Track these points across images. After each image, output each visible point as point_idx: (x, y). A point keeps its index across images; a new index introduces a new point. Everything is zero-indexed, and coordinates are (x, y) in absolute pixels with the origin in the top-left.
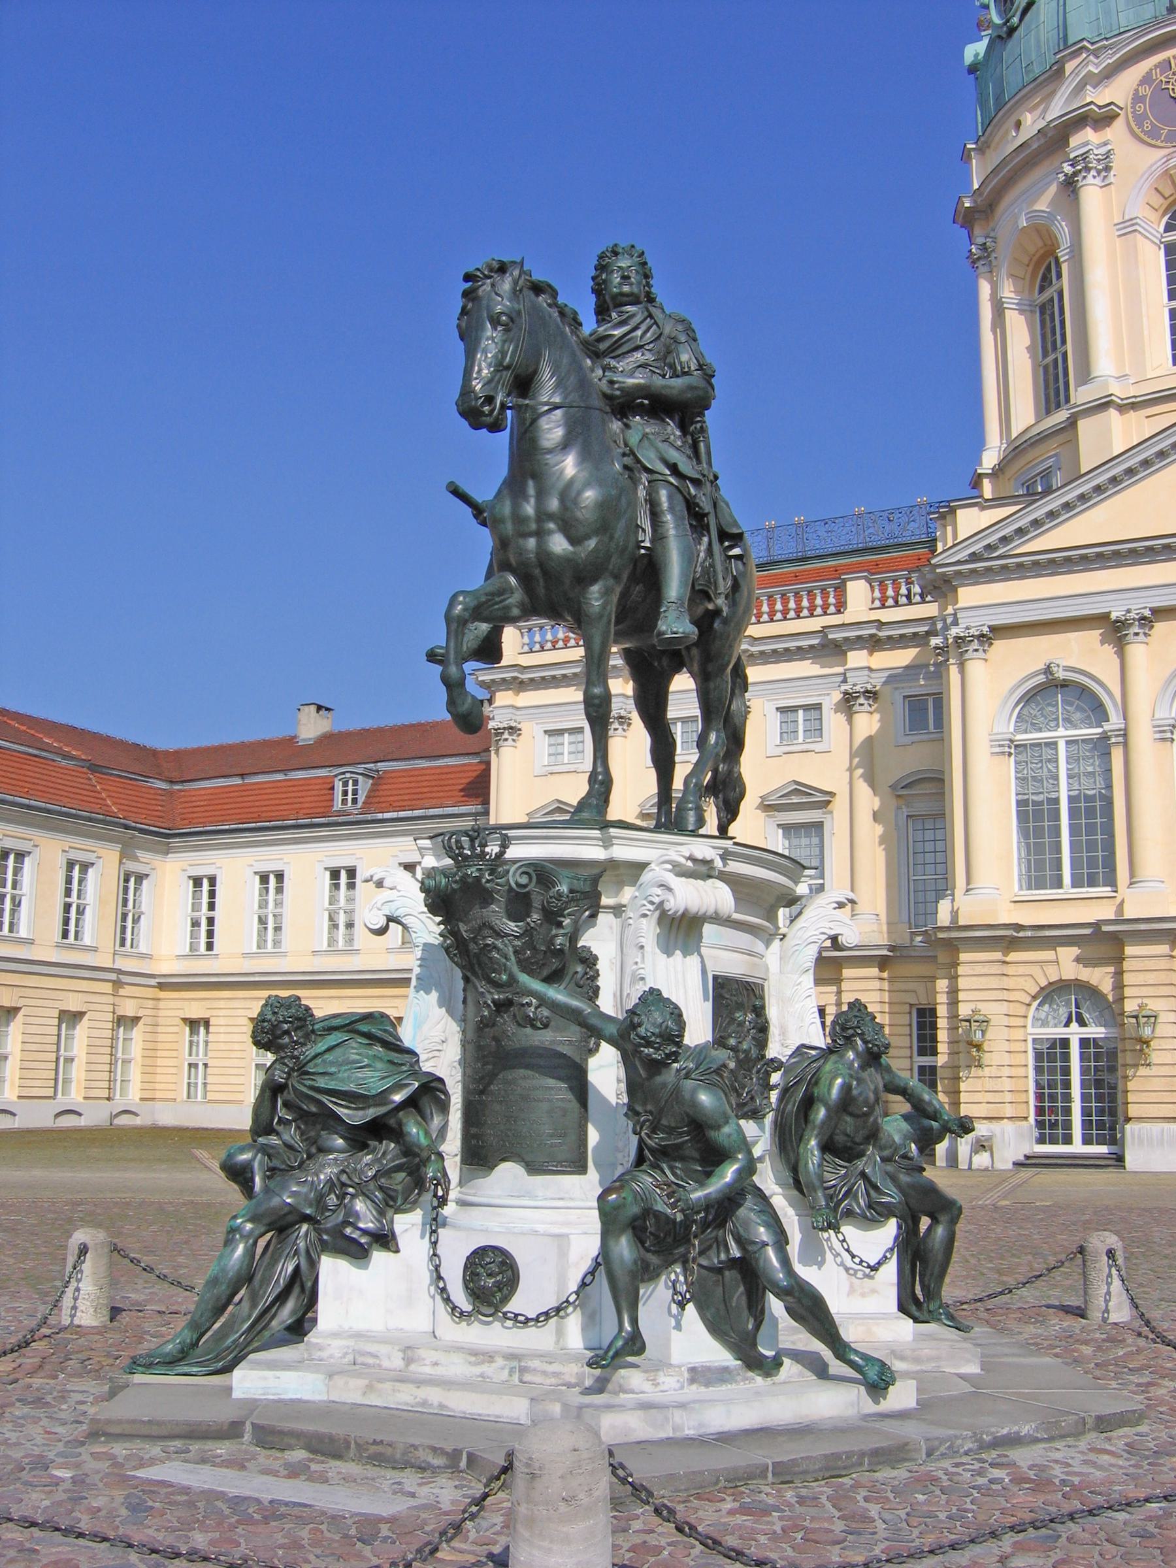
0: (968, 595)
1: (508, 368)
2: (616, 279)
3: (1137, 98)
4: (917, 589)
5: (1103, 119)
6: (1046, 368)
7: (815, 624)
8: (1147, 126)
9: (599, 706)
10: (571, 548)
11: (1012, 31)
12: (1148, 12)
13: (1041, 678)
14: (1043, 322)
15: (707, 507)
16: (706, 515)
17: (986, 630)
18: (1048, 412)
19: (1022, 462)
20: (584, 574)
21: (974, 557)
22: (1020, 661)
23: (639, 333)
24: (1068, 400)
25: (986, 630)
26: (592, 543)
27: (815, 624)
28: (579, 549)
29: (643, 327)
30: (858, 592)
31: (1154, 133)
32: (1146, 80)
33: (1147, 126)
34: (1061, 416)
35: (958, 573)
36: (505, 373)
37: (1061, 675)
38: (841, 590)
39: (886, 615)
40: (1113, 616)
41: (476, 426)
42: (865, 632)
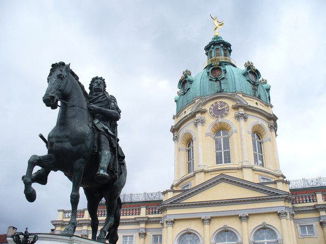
0: (169, 212)
1: (60, 90)
2: (96, 85)
3: (210, 109)
4: (157, 210)
5: (203, 112)
6: (189, 163)
7: (133, 217)
8: (212, 114)
9: (75, 198)
10: (72, 147)
11: (185, 94)
12: (213, 92)
13: (185, 232)
14: (188, 154)
15: (115, 146)
16: (115, 148)
17: (173, 220)
18: (189, 173)
19: (182, 183)
20: (77, 155)
21: (171, 203)
22: (181, 227)
23: (101, 98)
24: (193, 170)
25: (173, 220)
26: (79, 146)
27: (133, 217)
28: (74, 147)
29: (101, 97)
30: (143, 210)
31: (214, 116)
32: (212, 105)
33: (212, 114)
34: (192, 173)
35: (167, 206)
36: (59, 92)
37: (189, 231)
38: (139, 210)
39: (150, 216)
40: (202, 218)
41: (48, 105)
42: (145, 220)
